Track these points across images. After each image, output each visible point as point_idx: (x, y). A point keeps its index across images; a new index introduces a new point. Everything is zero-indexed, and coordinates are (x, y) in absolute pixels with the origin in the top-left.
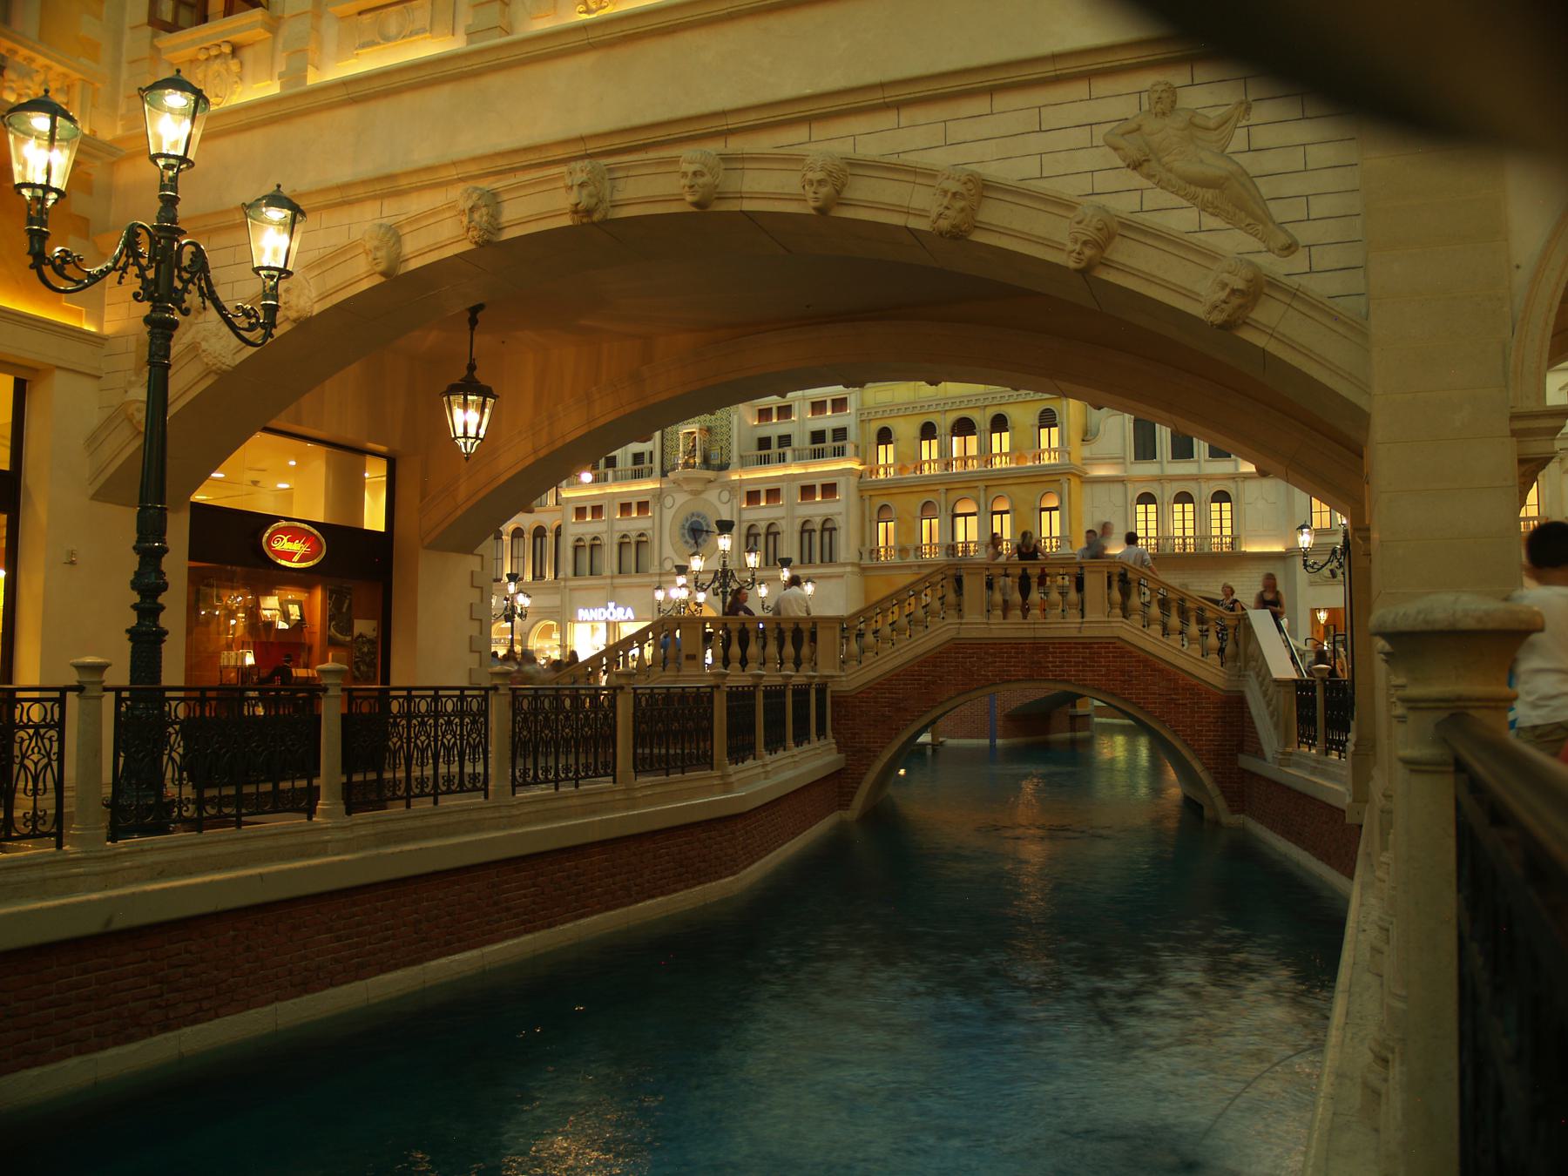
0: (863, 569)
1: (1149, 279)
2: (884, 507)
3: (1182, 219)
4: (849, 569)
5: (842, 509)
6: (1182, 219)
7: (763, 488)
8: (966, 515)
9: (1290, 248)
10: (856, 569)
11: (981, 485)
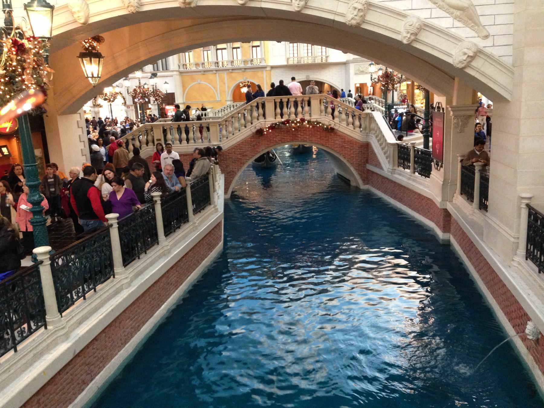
1: (433, 47)
3: (445, 22)
4: (175, 73)
6: (445, 22)
8: (222, 49)
9: (487, 37)
10: (178, 73)
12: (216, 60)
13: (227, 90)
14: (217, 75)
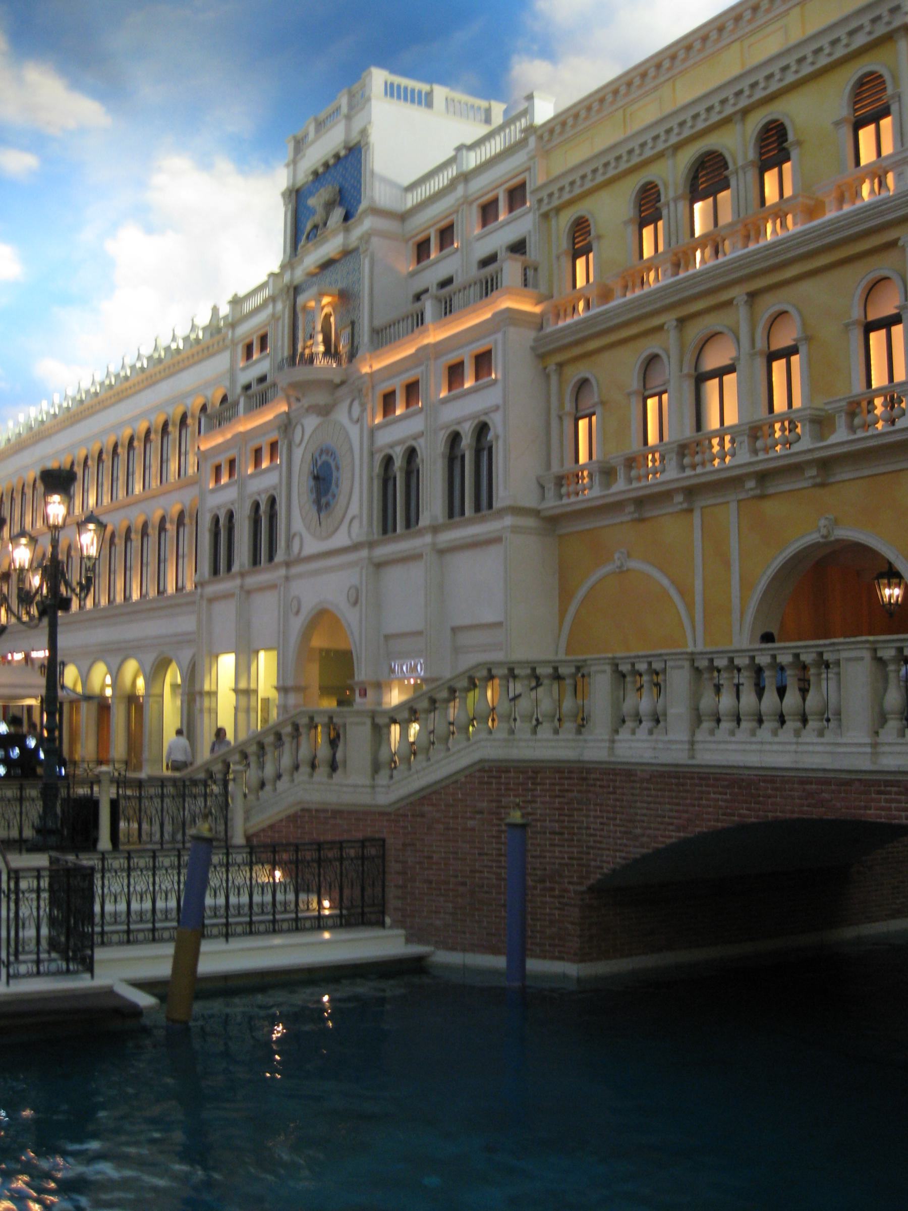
0: (552, 522)
2: (583, 384)
4: (508, 521)
5: (506, 400)
7: (398, 384)
10: (530, 522)
11: (738, 293)
12: (688, 432)
13: (736, 601)
14: (697, 517)
